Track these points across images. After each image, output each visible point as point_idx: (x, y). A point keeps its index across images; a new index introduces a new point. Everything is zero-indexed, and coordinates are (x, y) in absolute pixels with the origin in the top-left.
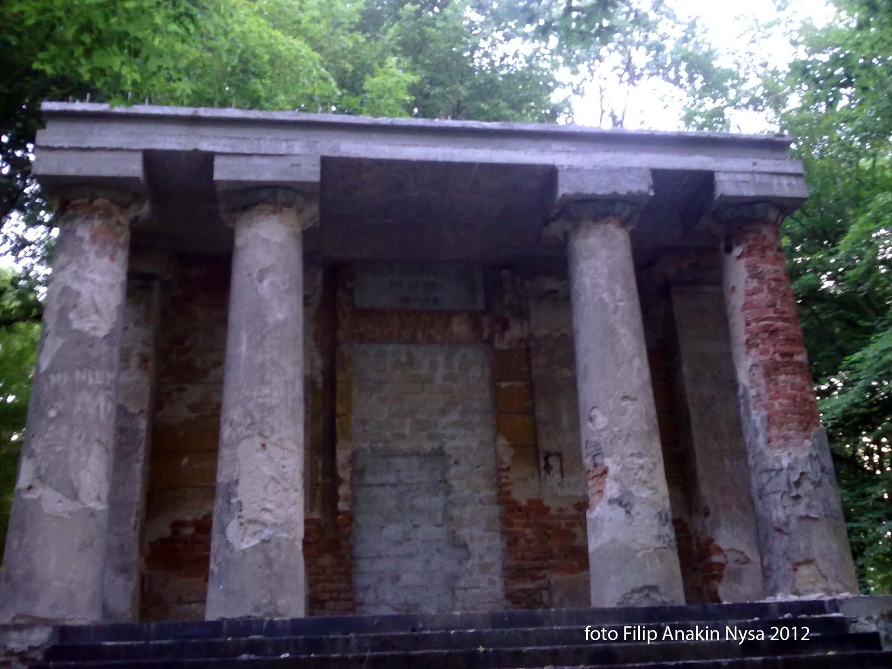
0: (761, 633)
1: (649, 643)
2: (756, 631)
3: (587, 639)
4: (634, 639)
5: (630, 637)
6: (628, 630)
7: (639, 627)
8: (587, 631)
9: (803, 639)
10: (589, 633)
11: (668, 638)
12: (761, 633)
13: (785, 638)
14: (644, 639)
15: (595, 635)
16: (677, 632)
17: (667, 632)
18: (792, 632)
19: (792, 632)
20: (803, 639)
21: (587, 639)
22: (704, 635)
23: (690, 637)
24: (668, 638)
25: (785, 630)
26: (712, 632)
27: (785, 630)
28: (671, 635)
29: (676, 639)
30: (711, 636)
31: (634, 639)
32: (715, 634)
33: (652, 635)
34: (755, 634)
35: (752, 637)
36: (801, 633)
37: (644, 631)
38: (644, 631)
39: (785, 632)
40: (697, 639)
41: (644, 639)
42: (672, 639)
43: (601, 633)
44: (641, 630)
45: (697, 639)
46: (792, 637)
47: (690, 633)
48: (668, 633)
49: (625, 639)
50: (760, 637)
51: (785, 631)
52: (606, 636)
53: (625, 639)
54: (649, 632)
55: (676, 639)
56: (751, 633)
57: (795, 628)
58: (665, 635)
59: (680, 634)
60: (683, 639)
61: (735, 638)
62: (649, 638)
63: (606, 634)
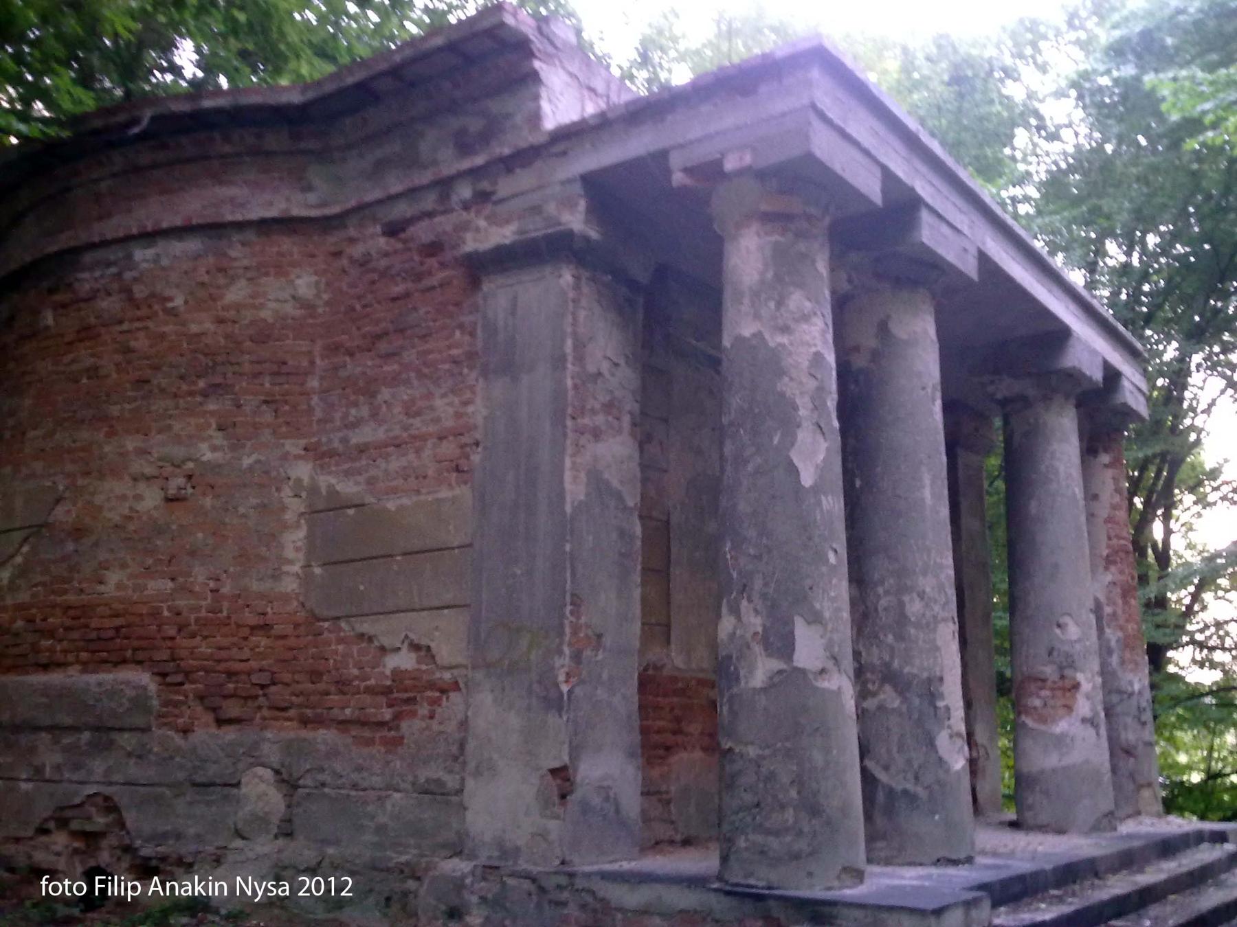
0: (284, 885)
1: (129, 900)
5: (103, 891)
6: (101, 882)
7: (116, 877)
8: (44, 883)
9: (343, 894)
10: (47, 886)
12: (284, 885)
15: (55, 889)
16: (168, 885)
18: (328, 884)
19: (328, 884)
20: (343, 894)
22: (206, 888)
23: (186, 891)
26: (217, 885)
28: (160, 889)
29: (168, 894)
31: (110, 894)
32: (221, 887)
34: (277, 887)
35: (272, 892)
38: (122, 883)
42: (162, 894)
43: (64, 886)
46: (328, 890)
47: (187, 885)
48: (156, 886)
50: (284, 891)
51: (318, 882)
52: (70, 890)
55: (168, 894)
56: (272, 885)
57: (332, 879)
58: (152, 888)
59: (172, 888)
61: (249, 893)
62: (130, 893)
63: (70, 887)
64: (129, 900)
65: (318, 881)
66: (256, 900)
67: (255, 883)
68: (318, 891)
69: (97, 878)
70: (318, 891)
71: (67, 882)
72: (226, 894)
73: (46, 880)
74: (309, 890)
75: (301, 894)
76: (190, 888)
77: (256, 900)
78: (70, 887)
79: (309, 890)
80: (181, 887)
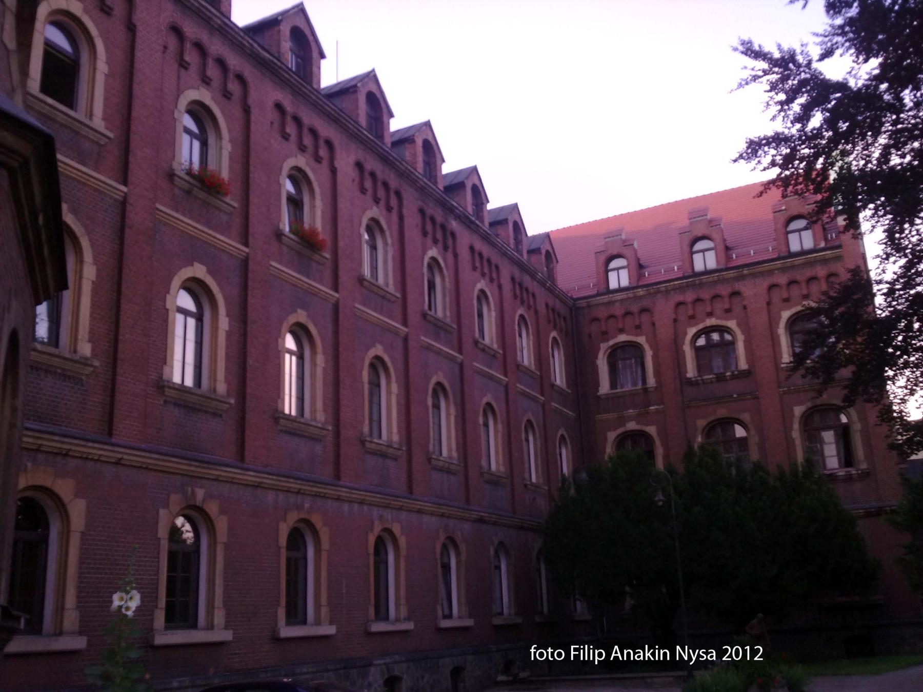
0: (712, 652)
1: (596, 663)
2: (707, 651)
3: (532, 659)
4: (582, 659)
6: (575, 650)
7: (586, 646)
8: (532, 650)
10: (535, 653)
12: (712, 652)
13: (737, 657)
14: (591, 659)
15: (541, 655)
16: (625, 652)
17: (616, 652)
18: (745, 652)
19: (745, 652)
21: (532, 659)
22: (653, 654)
23: (639, 657)
25: (737, 649)
26: (662, 652)
27: (737, 649)
28: (619, 655)
29: (625, 659)
30: (662, 654)
31: (582, 659)
32: (665, 654)
33: (600, 655)
34: (707, 654)
35: (703, 657)
36: (754, 652)
37: (591, 651)
38: (591, 651)
40: (647, 659)
41: (591, 659)
42: (621, 659)
43: (547, 653)
45: (647, 659)
47: (640, 652)
48: (616, 653)
49: (572, 659)
50: (712, 657)
51: (737, 650)
52: (553, 656)
53: (572, 659)
54: (597, 652)
55: (625, 659)
56: (703, 652)
57: (748, 647)
58: (613, 655)
59: (629, 654)
60: (632, 659)
61: (686, 658)
62: (597, 658)
63: (552, 654)
64: (596, 663)
65: (737, 649)
66: (691, 664)
67: (691, 651)
68: (737, 655)
69: (572, 647)
70: (737, 656)
71: (550, 650)
72: (668, 659)
73: (535, 648)
74: (730, 656)
75: (724, 659)
76: (642, 654)
77: (691, 664)
78: (552, 654)
79: (730, 656)
80: (635, 654)
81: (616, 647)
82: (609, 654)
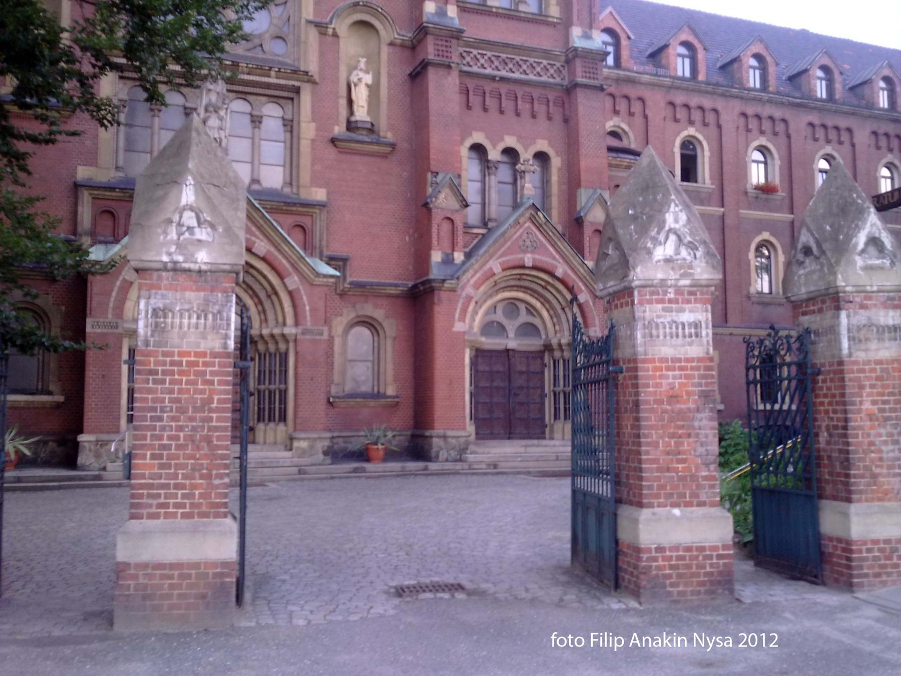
6: (595, 637)
8: (553, 637)
9: (771, 646)
10: (556, 640)
11: (635, 645)
15: (562, 642)
16: (644, 639)
17: (635, 639)
18: (760, 639)
19: (760, 639)
20: (771, 646)
22: (671, 641)
23: (657, 644)
24: (635, 645)
25: (753, 636)
26: (679, 639)
27: (753, 636)
28: (638, 642)
33: (619, 642)
34: (723, 641)
36: (769, 639)
39: (753, 639)
43: (568, 640)
44: (608, 636)
48: (635, 640)
50: (728, 643)
51: (753, 638)
52: (573, 643)
54: (616, 639)
58: (632, 642)
59: (647, 641)
61: (703, 645)
62: (616, 645)
68: (753, 644)
69: (592, 634)
70: (753, 644)
71: (570, 637)
74: (746, 643)
76: (660, 641)
79: (746, 643)
80: (653, 640)
81: (635, 634)
82: (627, 643)
